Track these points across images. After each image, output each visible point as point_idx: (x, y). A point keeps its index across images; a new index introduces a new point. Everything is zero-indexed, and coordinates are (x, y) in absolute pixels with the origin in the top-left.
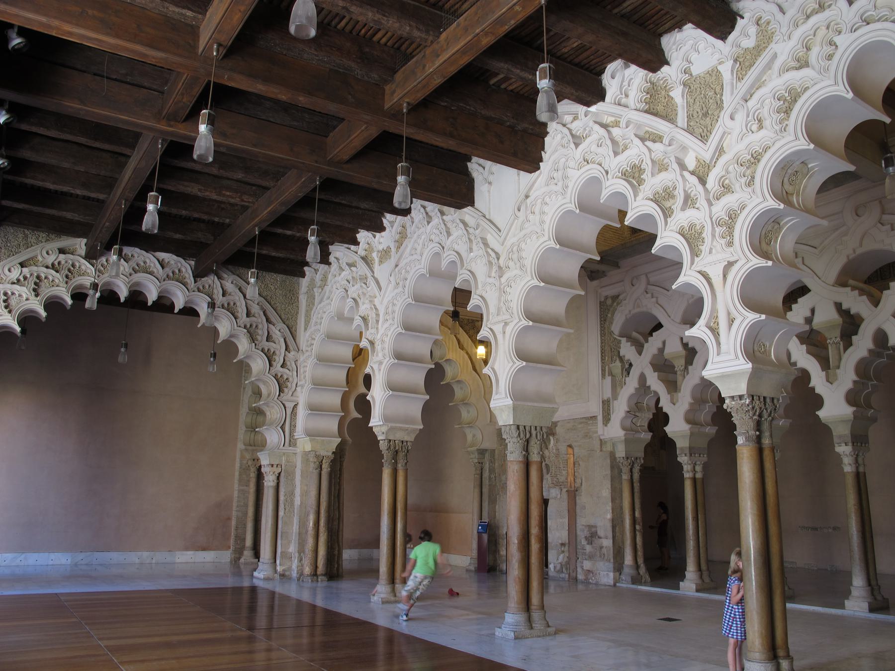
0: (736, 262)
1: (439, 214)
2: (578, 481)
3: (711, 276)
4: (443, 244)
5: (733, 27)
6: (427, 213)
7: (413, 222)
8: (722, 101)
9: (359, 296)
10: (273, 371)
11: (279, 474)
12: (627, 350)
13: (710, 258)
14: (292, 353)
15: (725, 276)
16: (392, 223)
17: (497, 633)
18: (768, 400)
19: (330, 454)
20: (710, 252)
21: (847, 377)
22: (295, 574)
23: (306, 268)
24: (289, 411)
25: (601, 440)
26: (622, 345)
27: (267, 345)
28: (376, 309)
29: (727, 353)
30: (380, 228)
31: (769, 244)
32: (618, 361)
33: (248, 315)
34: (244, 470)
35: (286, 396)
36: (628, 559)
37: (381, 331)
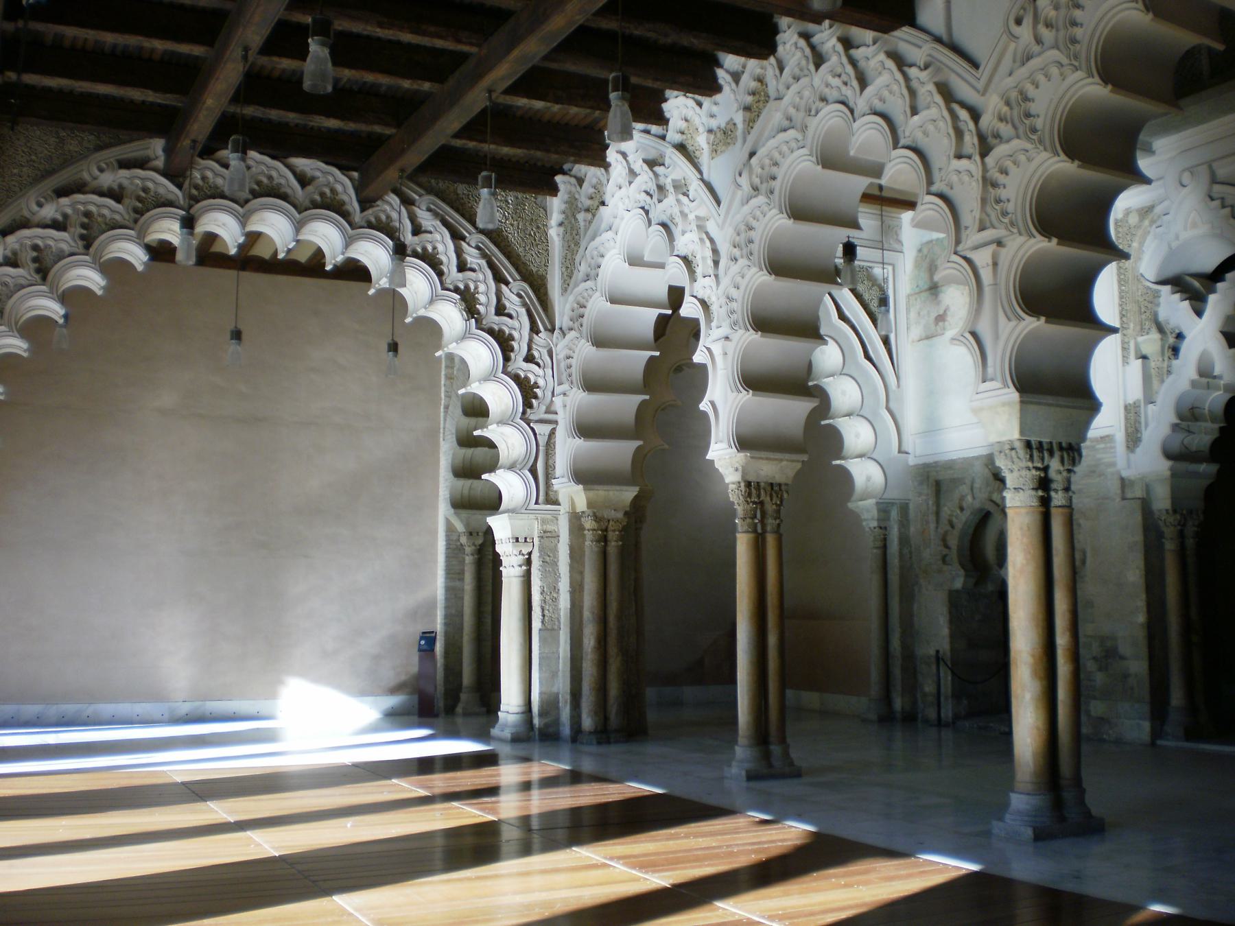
1: (840, 48)
2: (1078, 556)
4: (851, 104)
6: (813, 48)
7: (781, 69)
9: (672, 219)
11: (530, 554)
12: (1174, 308)
14: (543, 334)
16: (736, 77)
17: (995, 831)
19: (620, 515)
22: (566, 730)
23: (559, 179)
24: (542, 441)
25: (1122, 479)
26: (1162, 300)
27: (494, 320)
28: (712, 241)
30: (710, 87)
32: (1154, 330)
33: (462, 267)
34: (454, 551)
35: (538, 411)
36: (1177, 697)
37: (725, 281)
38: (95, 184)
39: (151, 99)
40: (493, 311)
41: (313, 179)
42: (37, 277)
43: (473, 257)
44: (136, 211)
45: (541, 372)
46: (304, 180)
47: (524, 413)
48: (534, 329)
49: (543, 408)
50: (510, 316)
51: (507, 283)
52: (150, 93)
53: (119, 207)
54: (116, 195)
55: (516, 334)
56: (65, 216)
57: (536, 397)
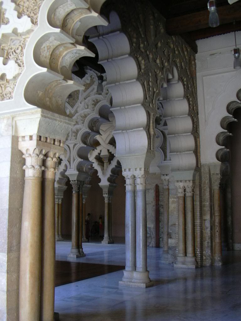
0: (77, 144)
3: (70, 146)
5: (84, 76)
8: (78, 96)
13: (70, 142)
15: (74, 148)
18: (82, 182)
20: (71, 140)
21: (109, 173)
29: (72, 168)
31: (86, 139)
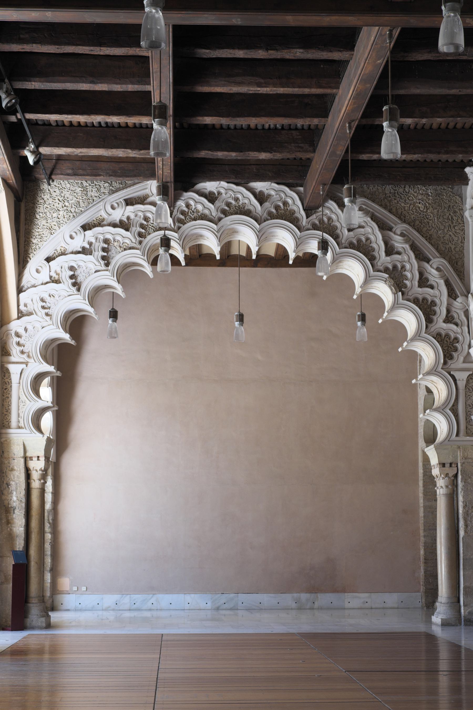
10: (434, 328)
11: (456, 476)
14: (459, 300)
33: (390, 251)
35: (458, 362)
38: (109, 219)
39: (131, 155)
40: (416, 283)
41: (269, 196)
42: (74, 289)
43: (398, 242)
44: (140, 235)
45: (459, 330)
46: (261, 198)
47: (445, 363)
48: (452, 295)
49: (461, 359)
50: (432, 287)
51: (428, 261)
52: (129, 151)
53: (128, 233)
54: (124, 225)
55: (437, 301)
56: (90, 244)
57: (456, 350)
